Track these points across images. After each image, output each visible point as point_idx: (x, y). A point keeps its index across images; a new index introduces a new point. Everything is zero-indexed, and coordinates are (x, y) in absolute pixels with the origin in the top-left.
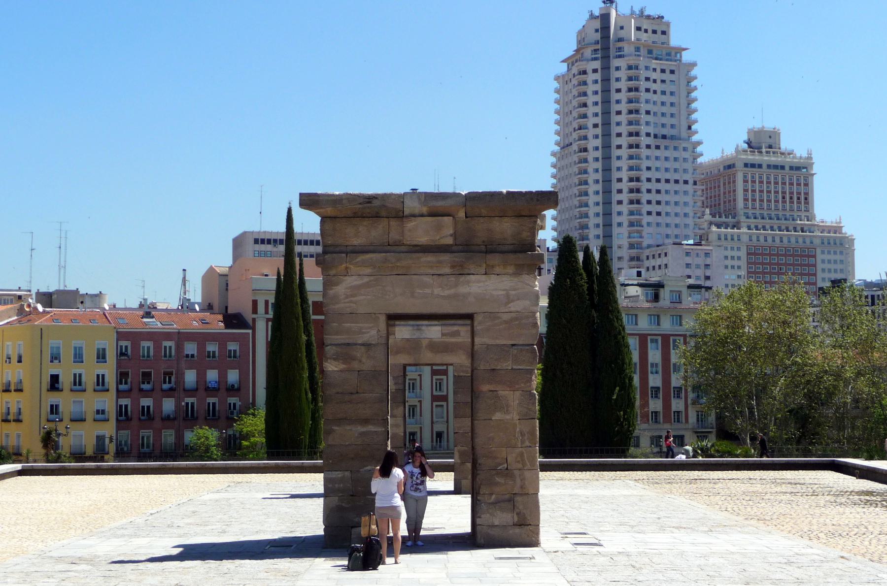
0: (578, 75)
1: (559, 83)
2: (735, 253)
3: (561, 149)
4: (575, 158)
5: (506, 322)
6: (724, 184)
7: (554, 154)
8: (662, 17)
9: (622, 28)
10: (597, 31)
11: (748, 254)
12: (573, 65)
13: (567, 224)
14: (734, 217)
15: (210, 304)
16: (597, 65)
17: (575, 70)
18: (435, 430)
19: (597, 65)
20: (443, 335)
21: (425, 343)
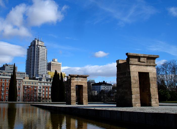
5: (153, 74)
7: (26, 60)
16: (33, 48)
17: (30, 48)
21: (79, 82)
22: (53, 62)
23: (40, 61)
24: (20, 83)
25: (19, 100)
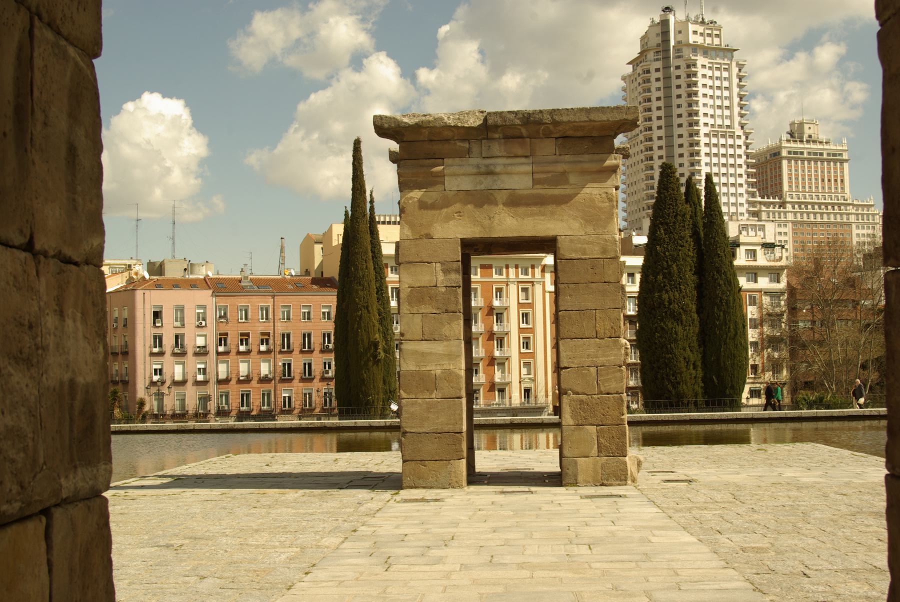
0: (642, 74)
1: (625, 82)
2: (783, 230)
3: (629, 140)
4: (642, 147)
6: (771, 169)
8: (715, 22)
9: (680, 32)
10: (658, 35)
11: (793, 230)
12: (638, 66)
13: (636, 205)
14: (780, 199)
15: (307, 270)
16: (659, 65)
17: (639, 70)
18: (524, 386)
19: (659, 65)
20: (535, 182)
21: (502, 196)
22: (792, 145)
23: (707, 140)
24: (529, 278)
25: (533, 386)
